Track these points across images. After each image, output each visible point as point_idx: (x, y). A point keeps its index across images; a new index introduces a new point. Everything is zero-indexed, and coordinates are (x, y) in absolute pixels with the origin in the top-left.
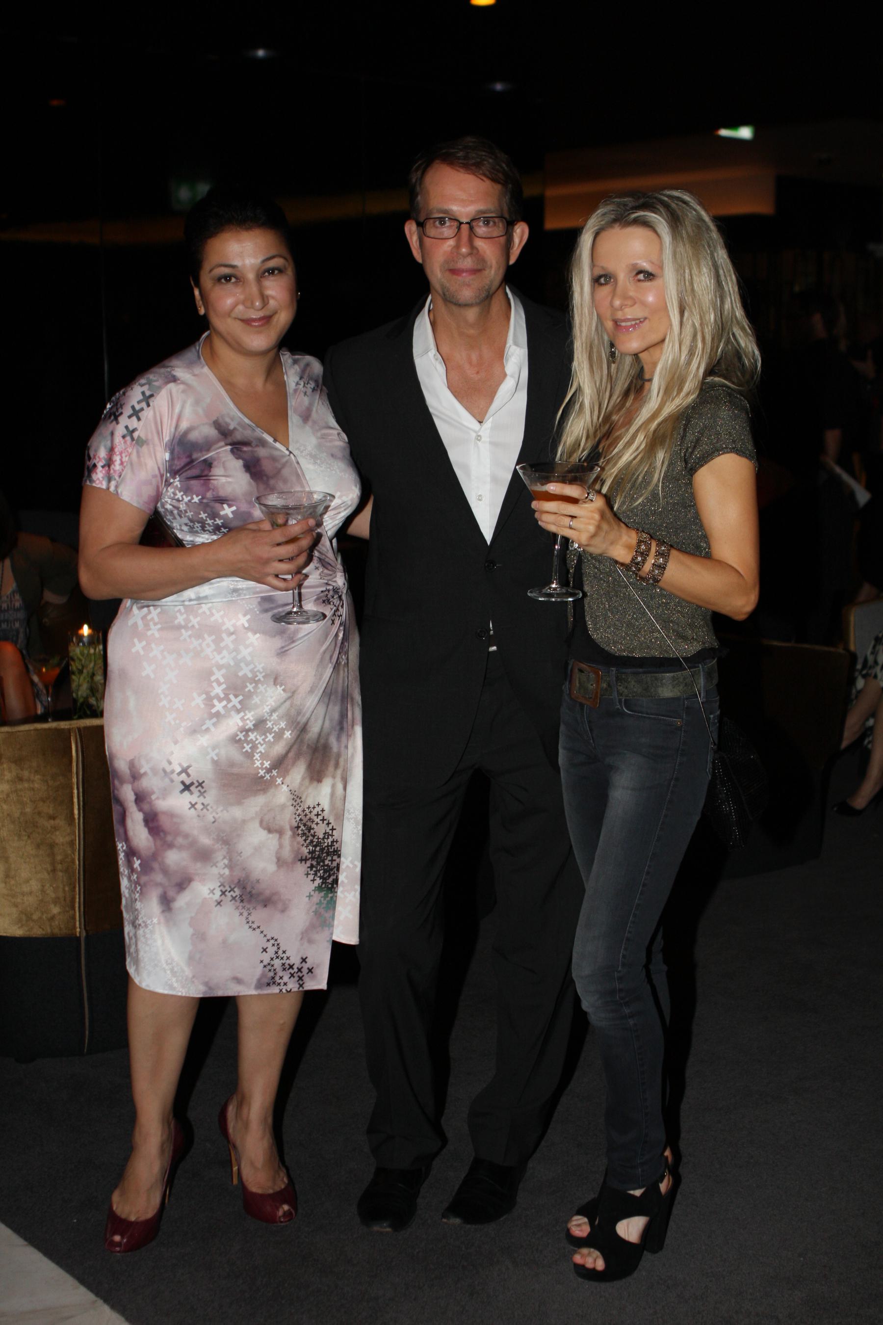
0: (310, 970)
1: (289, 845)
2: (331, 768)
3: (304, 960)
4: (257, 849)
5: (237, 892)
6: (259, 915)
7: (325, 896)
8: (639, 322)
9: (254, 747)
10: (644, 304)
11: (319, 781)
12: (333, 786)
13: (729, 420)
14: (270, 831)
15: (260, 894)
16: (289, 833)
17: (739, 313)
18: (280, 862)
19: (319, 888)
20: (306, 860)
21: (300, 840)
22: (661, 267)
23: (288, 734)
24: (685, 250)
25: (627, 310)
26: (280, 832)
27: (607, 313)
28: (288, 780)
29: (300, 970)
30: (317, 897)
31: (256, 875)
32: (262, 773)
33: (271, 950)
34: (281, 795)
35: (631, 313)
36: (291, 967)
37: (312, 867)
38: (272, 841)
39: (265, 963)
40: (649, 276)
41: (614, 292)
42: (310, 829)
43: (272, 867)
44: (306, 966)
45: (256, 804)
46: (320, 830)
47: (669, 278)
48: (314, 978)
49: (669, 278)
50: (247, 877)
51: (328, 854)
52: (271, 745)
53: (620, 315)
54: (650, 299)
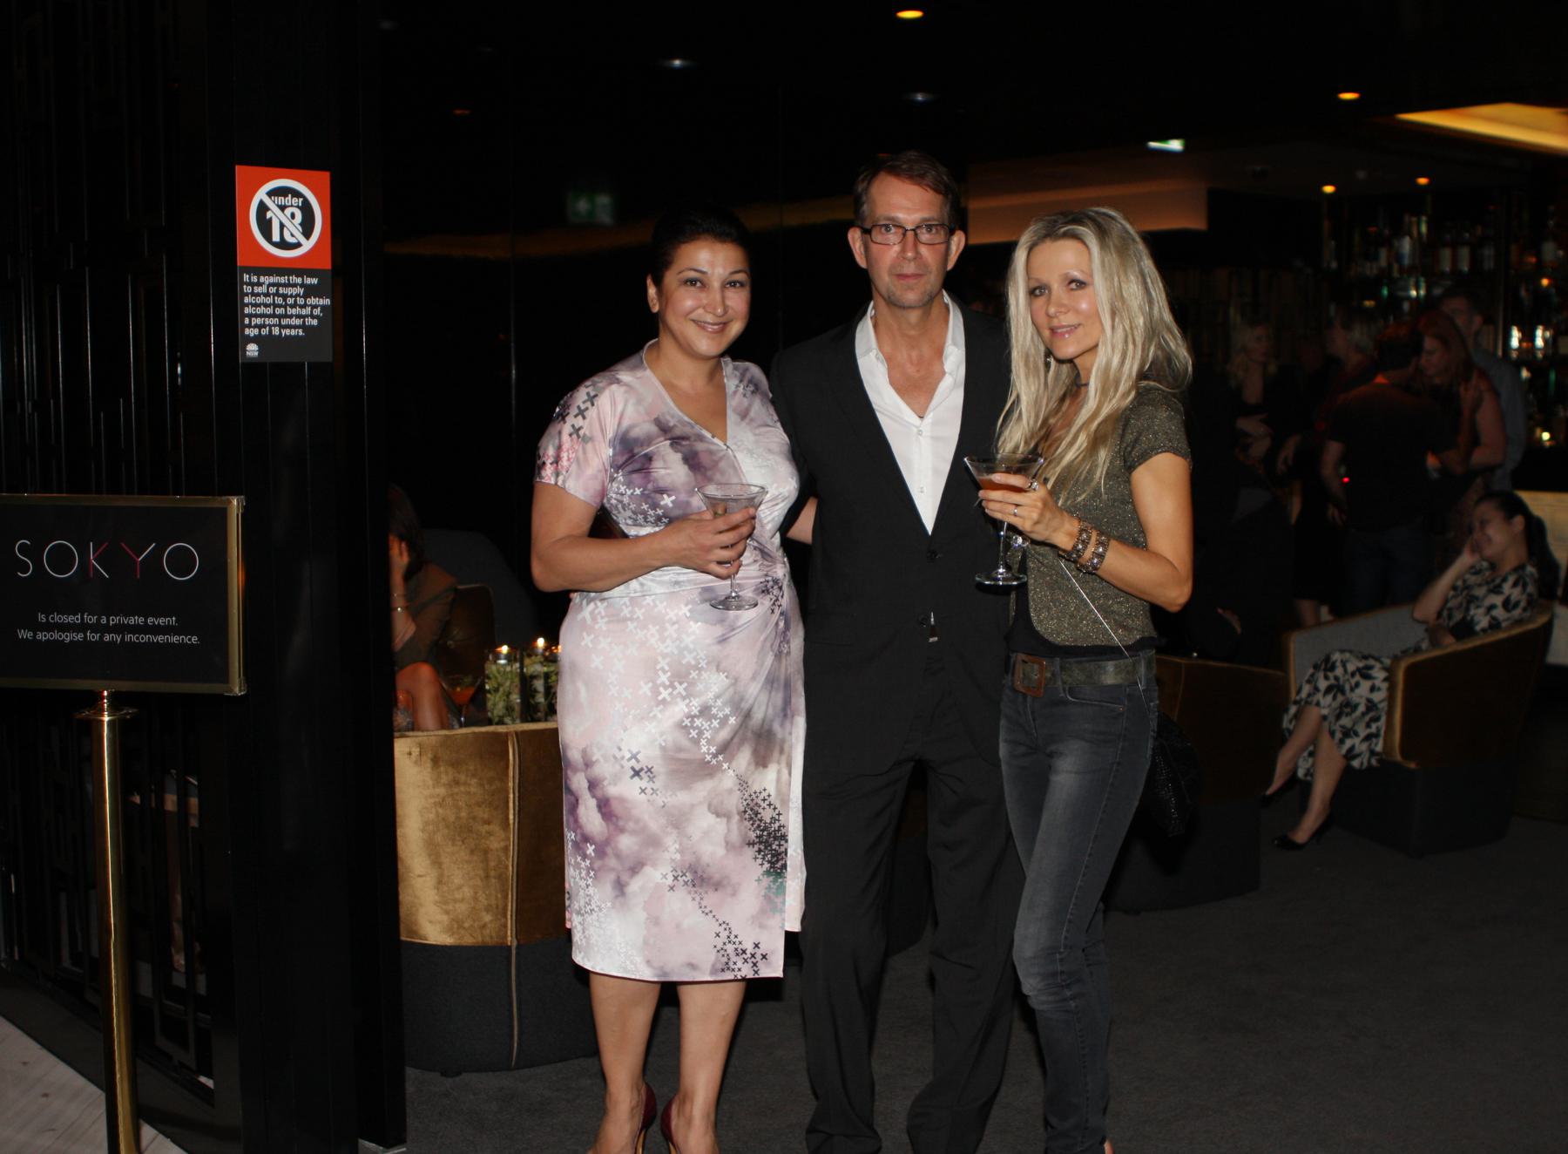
0: (764, 957)
1: (737, 829)
2: (776, 754)
3: (757, 946)
4: (706, 834)
5: (689, 877)
6: (711, 898)
7: (775, 881)
8: (1073, 328)
9: (700, 733)
10: (1077, 312)
11: (765, 766)
12: (779, 772)
13: (1166, 421)
14: (718, 815)
15: (710, 878)
16: (737, 818)
17: (1168, 317)
18: (729, 845)
19: (768, 873)
20: (753, 844)
21: (748, 824)
22: (1091, 276)
23: (732, 720)
24: (1113, 259)
25: (1062, 317)
26: (728, 816)
27: (1042, 320)
28: (734, 764)
29: (753, 956)
30: (766, 881)
31: (706, 859)
32: (708, 758)
33: (724, 934)
34: (728, 780)
35: (1067, 319)
36: (744, 952)
37: (759, 851)
38: (720, 826)
39: (720, 946)
40: (1081, 284)
41: (1048, 302)
42: (757, 814)
43: (721, 851)
44: (759, 953)
45: (703, 789)
46: (767, 815)
47: (1100, 285)
48: (769, 965)
49: (1100, 285)
50: (698, 859)
51: (775, 838)
52: (717, 731)
53: (1055, 322)
54: (1084, 306)
